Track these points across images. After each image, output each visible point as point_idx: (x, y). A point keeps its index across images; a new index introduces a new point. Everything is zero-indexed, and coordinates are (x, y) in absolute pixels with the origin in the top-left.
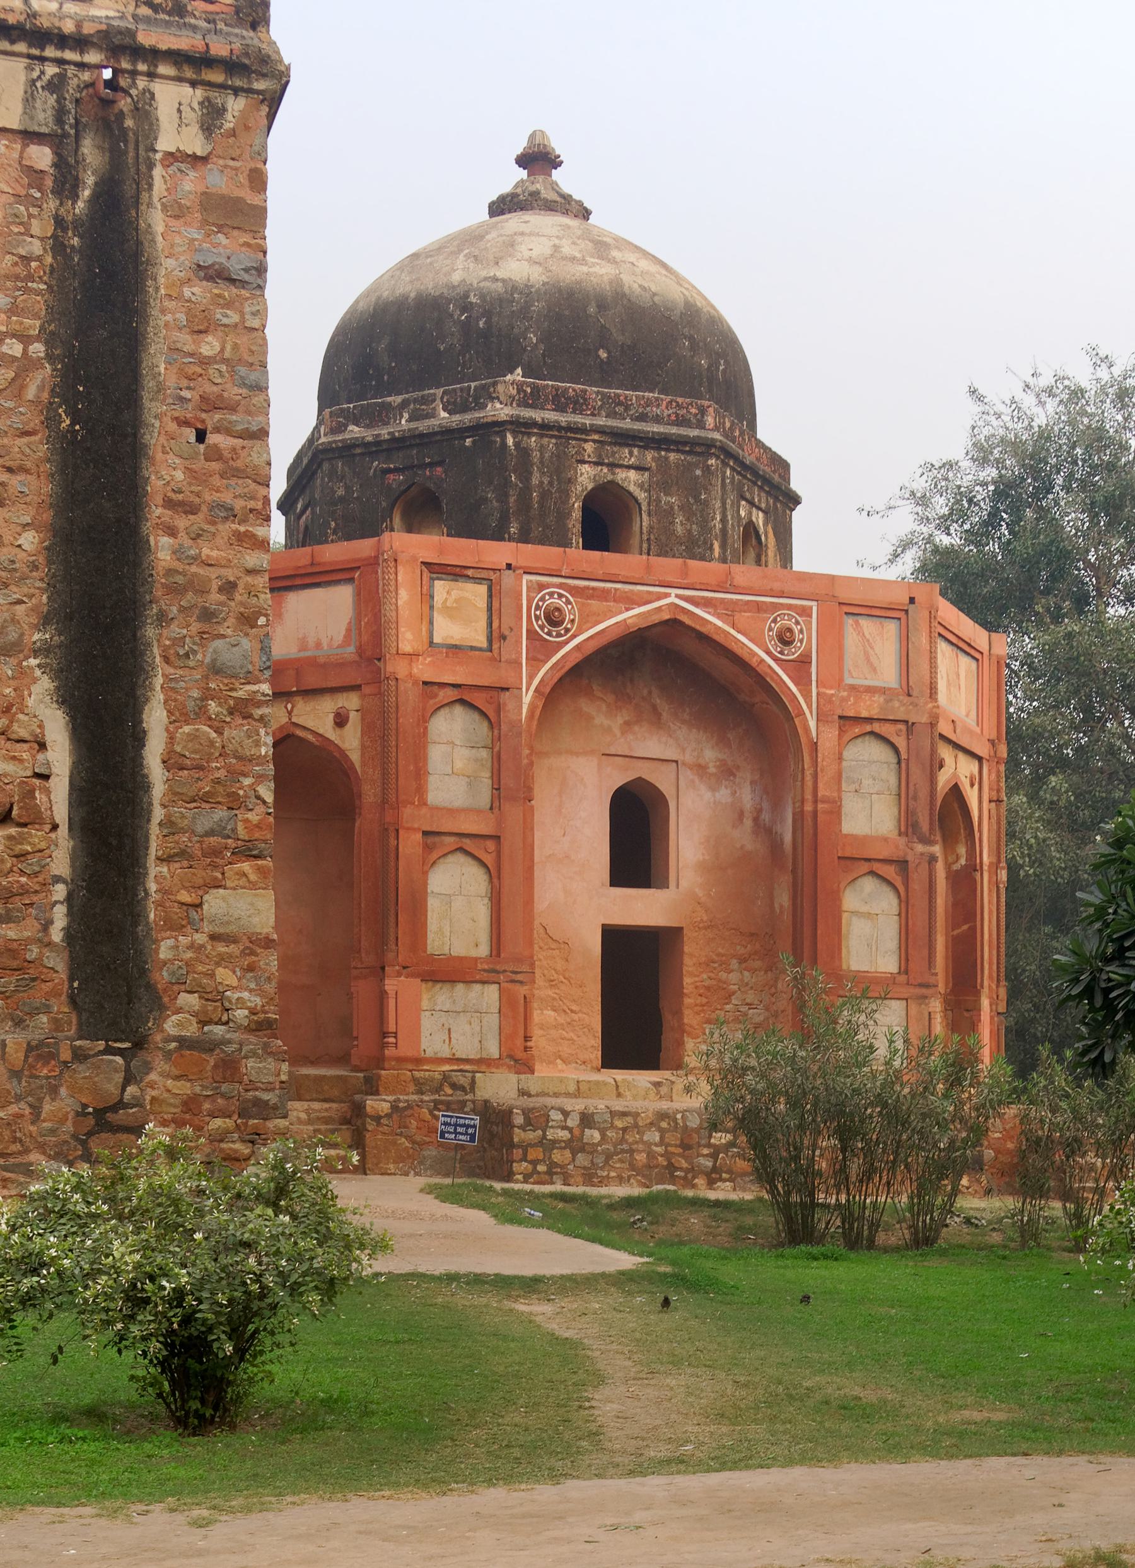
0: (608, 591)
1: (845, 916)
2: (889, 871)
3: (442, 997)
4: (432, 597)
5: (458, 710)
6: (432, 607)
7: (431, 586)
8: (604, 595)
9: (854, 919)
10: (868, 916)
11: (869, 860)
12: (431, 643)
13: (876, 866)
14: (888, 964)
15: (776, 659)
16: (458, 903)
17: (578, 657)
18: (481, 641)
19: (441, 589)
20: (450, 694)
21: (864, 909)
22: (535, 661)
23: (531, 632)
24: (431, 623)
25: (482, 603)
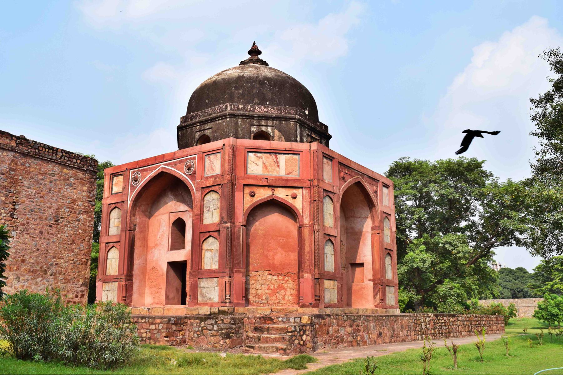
0: (147, 169)
1: (203, 251)
2: (216, 234)
3: (107, 286)
4: (112, 182)
5: (116, 209)
6: (112, 185)
7: (113, 180)
8: (144, 170)
9: (206, 252)
10: (210, 250)
11: (209, 232)
12: (112, 194)
13: (211, 234)
14: (215, 266)
15: (187, 175)
16: (113, 260)
17: (141, 188)
18: (121, 190)
19: (115, 180)
20: (113, 206)
21: (209, 248)
22: (132, 192)
23: (131, 185)
24: (112, 188)
25: (122, 180)
